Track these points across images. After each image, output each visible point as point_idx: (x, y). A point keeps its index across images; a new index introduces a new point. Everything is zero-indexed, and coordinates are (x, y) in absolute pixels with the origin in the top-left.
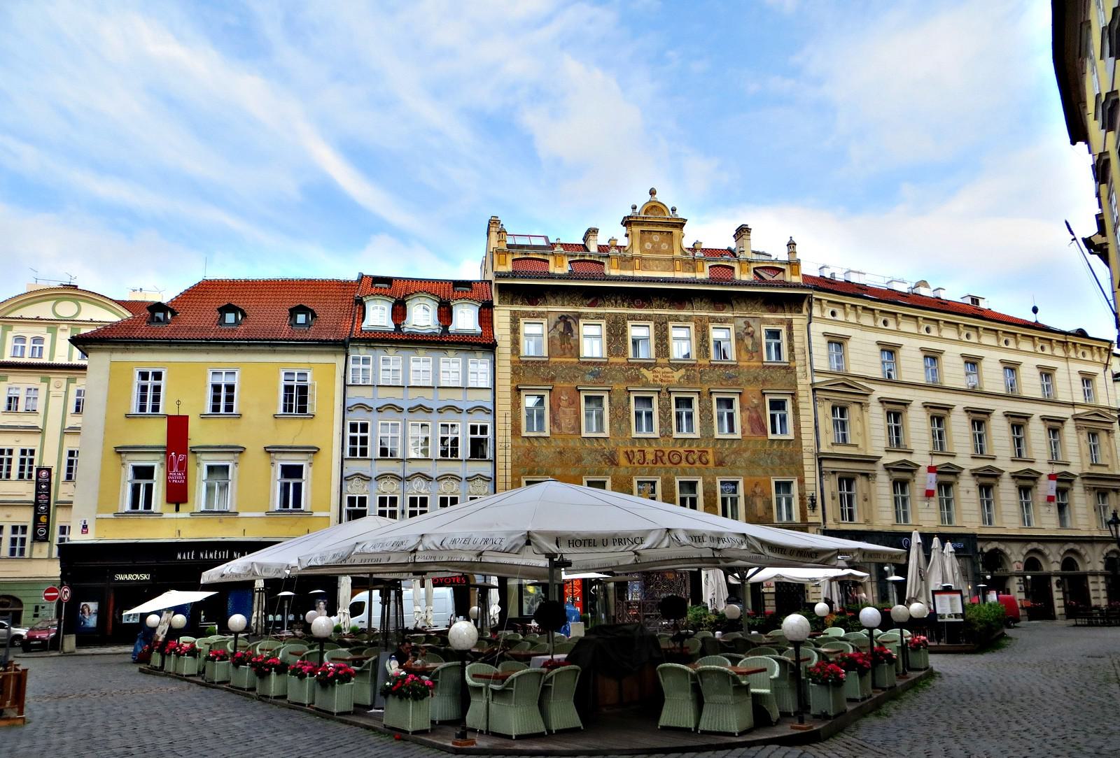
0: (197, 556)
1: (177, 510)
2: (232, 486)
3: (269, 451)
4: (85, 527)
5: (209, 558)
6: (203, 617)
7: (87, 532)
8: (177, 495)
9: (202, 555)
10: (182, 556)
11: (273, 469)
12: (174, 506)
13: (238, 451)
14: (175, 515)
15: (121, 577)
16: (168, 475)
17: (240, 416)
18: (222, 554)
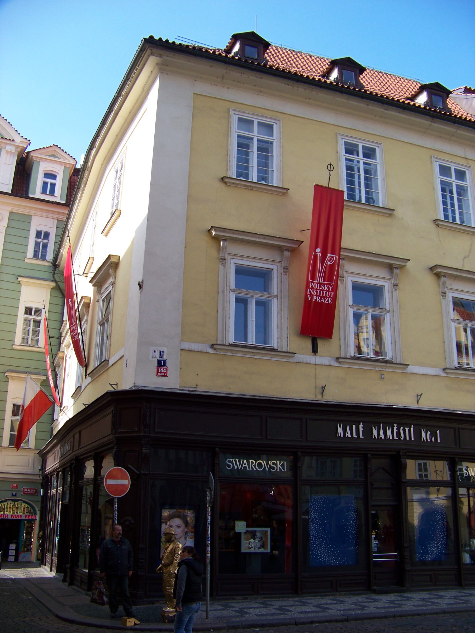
0: (368, 432)
1: (315, 350)
2: (392, 323)
3: (437, 272)
4: (162, 363)
5: (386, 439)
6: (375, 542)
7: (166, 375)
8: (317, 323)
9: (375, 432)
10: (345, 432)
11: (443, 301)
12: (308, 344)
13: (394, 266)
14: (312, 359)
15: (237, 464)
16: (307, 286)
17: (389, 212)
18: (404, 431)
